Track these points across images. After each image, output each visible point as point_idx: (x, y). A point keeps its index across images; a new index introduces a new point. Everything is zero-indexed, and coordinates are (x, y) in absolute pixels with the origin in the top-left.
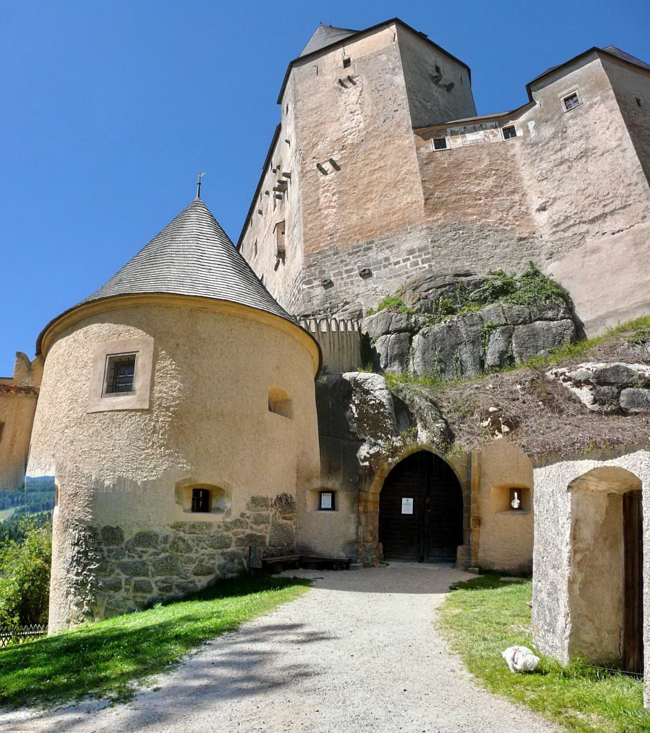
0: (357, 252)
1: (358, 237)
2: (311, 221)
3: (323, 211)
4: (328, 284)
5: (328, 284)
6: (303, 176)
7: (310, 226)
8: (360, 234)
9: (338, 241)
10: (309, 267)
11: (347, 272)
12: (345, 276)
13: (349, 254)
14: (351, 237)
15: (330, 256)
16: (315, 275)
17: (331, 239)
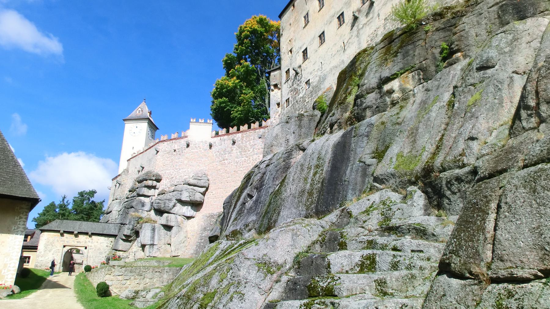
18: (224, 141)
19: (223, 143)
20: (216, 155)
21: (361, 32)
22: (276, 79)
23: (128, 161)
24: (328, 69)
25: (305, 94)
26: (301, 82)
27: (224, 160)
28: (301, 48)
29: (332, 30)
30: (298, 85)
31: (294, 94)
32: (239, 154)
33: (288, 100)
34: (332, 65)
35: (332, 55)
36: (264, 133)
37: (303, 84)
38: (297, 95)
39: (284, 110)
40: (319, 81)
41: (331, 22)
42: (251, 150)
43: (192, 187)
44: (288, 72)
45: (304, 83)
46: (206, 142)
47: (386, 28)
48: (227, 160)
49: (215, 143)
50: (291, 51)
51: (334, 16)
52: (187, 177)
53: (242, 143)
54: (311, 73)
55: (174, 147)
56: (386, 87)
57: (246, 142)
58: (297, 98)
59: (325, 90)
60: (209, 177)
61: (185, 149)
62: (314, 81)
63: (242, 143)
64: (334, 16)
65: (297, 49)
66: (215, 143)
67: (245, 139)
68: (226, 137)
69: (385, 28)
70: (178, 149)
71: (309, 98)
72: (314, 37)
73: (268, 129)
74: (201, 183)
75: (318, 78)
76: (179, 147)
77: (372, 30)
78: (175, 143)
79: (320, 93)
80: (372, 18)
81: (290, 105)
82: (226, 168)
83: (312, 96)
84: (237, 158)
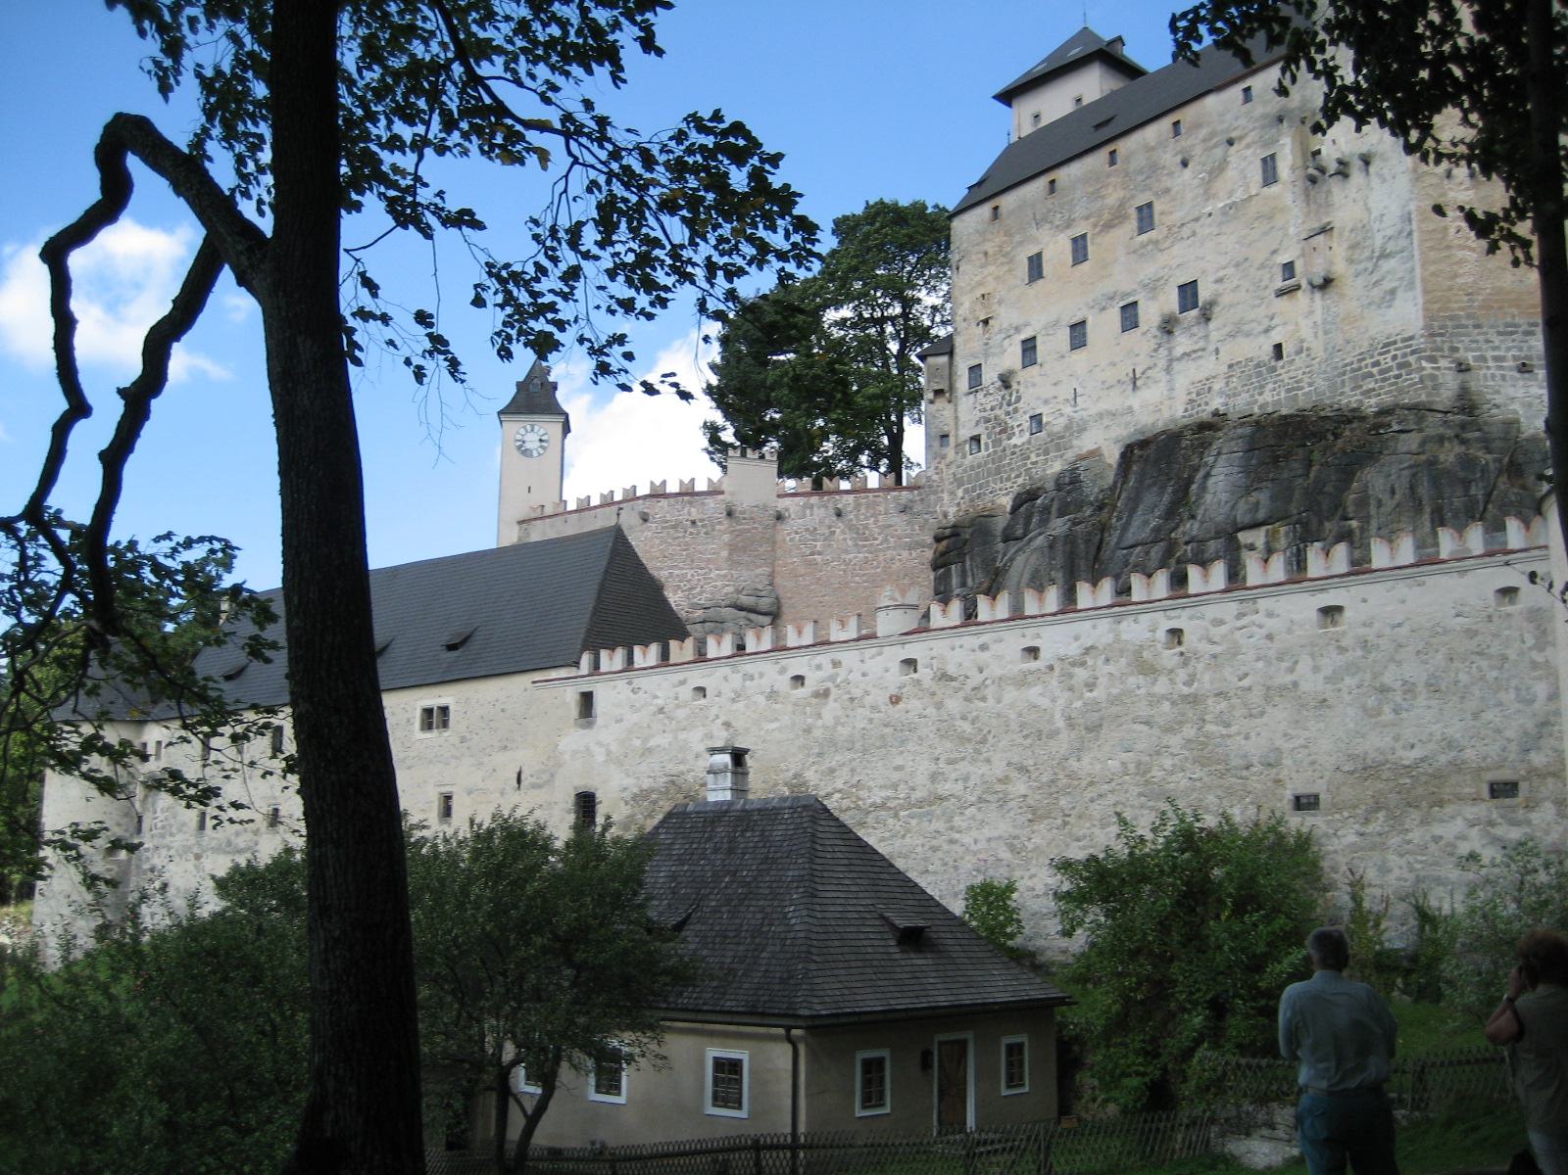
0: (1512, 333)
1: (1515, 311)
2: (1434, 262)
3: (1454, 252)
4: (1462, 368)
5: (1462, 368)
6: (1417, 179)
7: (1433, 268)
8: (1518, 306)
9: (1481, 308)
10: (1432, 335)
11: (1496, 359)
12: (1491, 363)
13: (1499, 333)
14: (1501, 308)
15: (1466, 327)
16: (1442, 350)
17: (1469, 300)
18: (812, 507)
19: (808, 512)
20: (791, 540)
21: (1177, 366)
22: (942, 377)
23: (520, 523)
24: (1093, 411)
25: (1029, 442)
26: (1016, 410)
27: (812, 554)
28: (1017, 330)
29: (1104, 325)
30: (1008, 414)
31: (998, 430)
32: (850, 543)
33: (976, 439)
34: (1103, 406)
35: (1103, 382)
36: (911, 501)
37: (1024, 420)
38: (1004, 436)
39: (964, 457)
40: (1067, 427)
41: (1104, 309)
42: (880, 538)
43: (743, 613)
44: (975, 370)
45: (1027, 417)
46: (765, 508)
47: (1232, 385)
48: (819, 553)
49: (787, 510)
50: (986, 322)
51: (1112, 298)
52: (730, 589)
53: (858, 519)
54: (1046, 402)
55: (689, 514)
56: (1244, 537)
57: (867, 518)
58: (1005, 443)
59: (1084, 451)
60: (780, 592)
61: (720, 523)
62: (1054, 422)
63: (858, 519)
64: (1112, 298)
65: (1005, 325)
66: (787, 510)
67: (863, 511)
68: (814, 500)
69: (1227, 384)
70: (702, 520)
71: (1038, 455)
72: (1057, 322)
73: (920, 494)
74: (765, 603)
75: (1062, 421)
76: (700, 516)
77: (1202, 375)
78: (690, 503)
79: (1070, 455)
80: (1204, 350)
81: (983, 453)
82: (818, 575)
83: (1046, 452)
84: (846, 552)
